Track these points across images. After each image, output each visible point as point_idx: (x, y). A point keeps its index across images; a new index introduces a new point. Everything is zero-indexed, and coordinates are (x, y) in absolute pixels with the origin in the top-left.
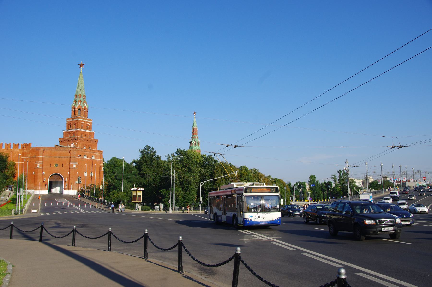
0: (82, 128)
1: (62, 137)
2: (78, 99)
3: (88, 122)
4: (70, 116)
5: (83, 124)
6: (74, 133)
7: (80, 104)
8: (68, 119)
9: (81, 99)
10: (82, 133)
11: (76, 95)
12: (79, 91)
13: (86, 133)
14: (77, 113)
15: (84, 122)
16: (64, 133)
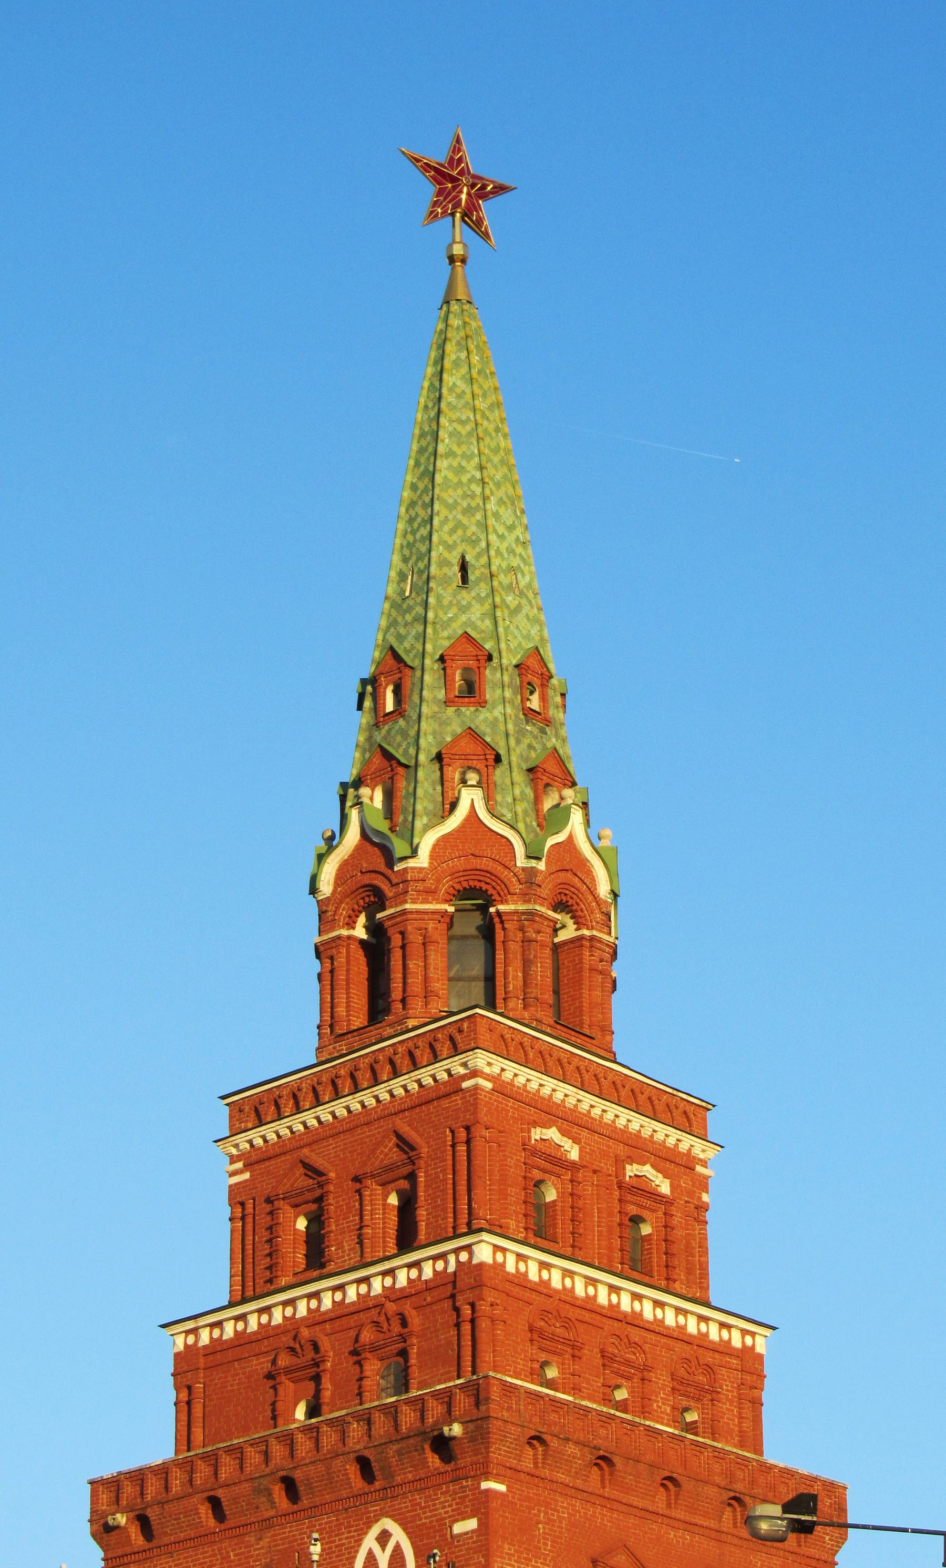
0: (541, 1230)
1: (149, 1437)
2: (437, 722)
3: (640, 1148)
4: (285, 1033)
5: (554, 1161)
6: (386, 1333)
7: (470, 798)
8: (250, 1109)
9: (496, 716)
10: (560, 1325)
11: (394, 669)
12: (444, 592)
13: (621, 1346)
14: (437, 980)
15: (572, 1122)
16: (187, 1367)
